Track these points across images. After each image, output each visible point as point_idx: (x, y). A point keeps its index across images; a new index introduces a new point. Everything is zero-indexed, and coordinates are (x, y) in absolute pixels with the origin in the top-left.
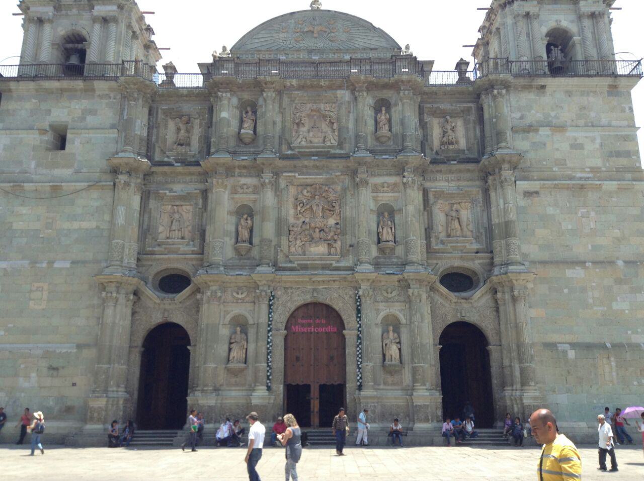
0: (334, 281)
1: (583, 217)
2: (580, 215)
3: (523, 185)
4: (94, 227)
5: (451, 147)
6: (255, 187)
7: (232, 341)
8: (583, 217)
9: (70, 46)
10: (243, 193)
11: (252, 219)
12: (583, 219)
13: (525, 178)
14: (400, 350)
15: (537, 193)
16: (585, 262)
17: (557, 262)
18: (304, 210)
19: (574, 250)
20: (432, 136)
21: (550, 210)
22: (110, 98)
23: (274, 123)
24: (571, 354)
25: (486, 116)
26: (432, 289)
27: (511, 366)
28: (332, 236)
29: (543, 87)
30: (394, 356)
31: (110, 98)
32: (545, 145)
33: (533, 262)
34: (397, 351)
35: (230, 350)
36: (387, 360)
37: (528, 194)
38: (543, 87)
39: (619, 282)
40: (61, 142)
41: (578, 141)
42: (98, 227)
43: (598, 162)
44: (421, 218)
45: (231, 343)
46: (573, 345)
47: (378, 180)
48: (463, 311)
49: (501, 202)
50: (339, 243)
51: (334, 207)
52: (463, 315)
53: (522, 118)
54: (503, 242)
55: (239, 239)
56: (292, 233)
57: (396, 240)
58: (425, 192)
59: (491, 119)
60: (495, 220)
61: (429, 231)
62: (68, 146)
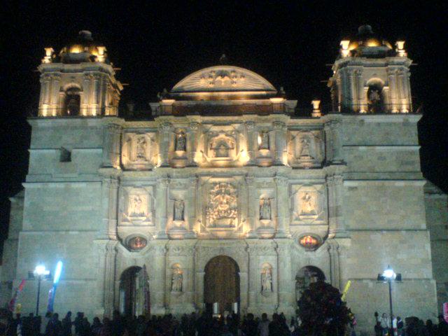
1: (383, 203)
2: (381, 202)
3: (347, 184)
6: (185, 185)
9: (69, 93)
13: (350, 180)
14: (271, 283)
15: (356, 188)
21: (364, 199)
24: (371, 284)
33: (352, 230)
37: (351, 189)
38: (362, 120)
39: (402, 242)
40: (66, 157)
41: (383, 156)
43: (394, 168)
45: (172, 279)
47: (260, 180)
60: (331, 205)
62: (72, 159)
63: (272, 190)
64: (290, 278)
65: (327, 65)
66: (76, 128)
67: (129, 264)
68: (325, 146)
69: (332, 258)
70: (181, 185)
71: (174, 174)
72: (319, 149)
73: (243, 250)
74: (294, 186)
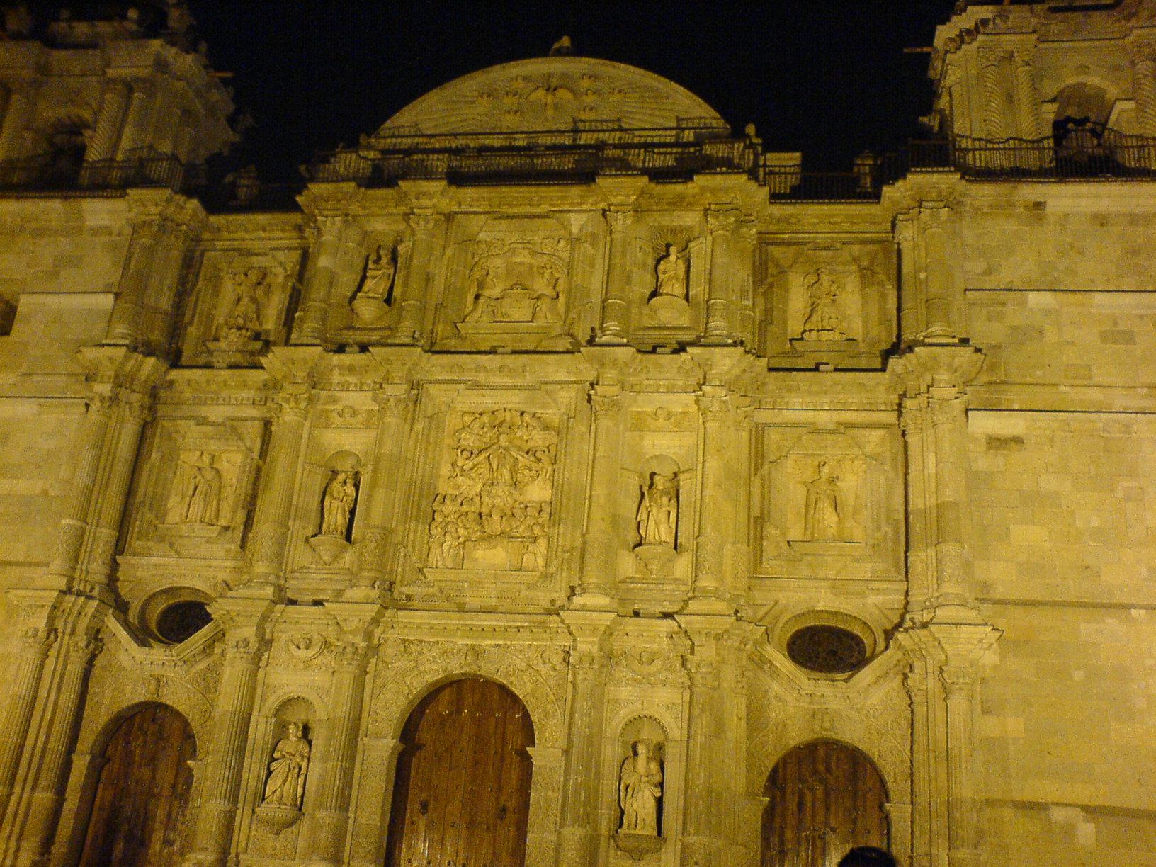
0: (518, 628)
3: (985, 424)
4: (38, 491)
5: (825, 336)
7: (276, 755)
8: (1128, 499)
9: (60, 139)
10: (347, 427)
11: (357, 486)
12: (1130, 505)
14: (660, 801)
15: (1018, 440)
16: (1128, 607)
17: (1056, 604)
18: (471, 465)
19: (1103, 577)
20: (785, 312)
21: (1049, 483)
22: (111, 233)
23: (428, 279)
24: (1087, 831)
25: (907, 268)
26: (760, 662)
27: (930, 855)
28: (531, 528)
29: (1039, 205)
30: (642, 814)
31: (111, 233)
32: (1041, 332)
34: (652, 804)
35: (270, 773)
36: (625, 825)
37: (997, 443)
38: (1039, 205)
41: (1122, 327)
42: (45, 493)
44: (742, 491)
46: (1091, 811)
48: (827, 718)
49: (931, 459)
50: (542, 543)
51: (539, 460)
52: (827, 725)
53: (988, 272)
54: (931, 552)
55: (325, 525)
56: (438, 518)
57: (679, 541)
58: (759, 434)
59: (916, 272)
60: (917, 503)
61: (758, 524)
63: (689, 439)
64: (741, 784)
65: (905, 50)
66: (40, 233)
67: (136, 694)
68: (899, 297)
69: (920, 710)
70: (355, 413)
71: (336, 378)
72: (873, 308)
73: (557, 659)
74: (773, 436)
